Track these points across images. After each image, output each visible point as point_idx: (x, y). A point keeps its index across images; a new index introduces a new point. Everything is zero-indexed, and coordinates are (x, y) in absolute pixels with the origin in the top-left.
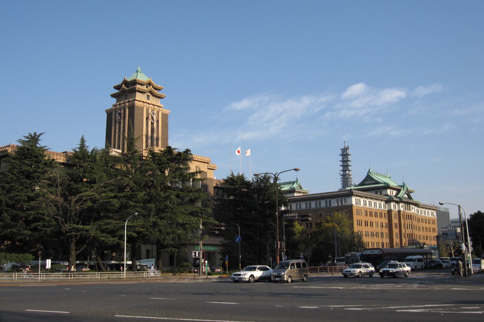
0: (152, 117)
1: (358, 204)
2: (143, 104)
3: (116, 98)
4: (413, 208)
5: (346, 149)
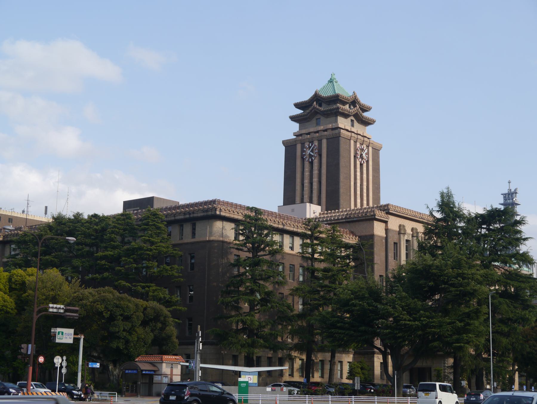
0: (361, 155)
2: (349, 134)
5: (513, 194)
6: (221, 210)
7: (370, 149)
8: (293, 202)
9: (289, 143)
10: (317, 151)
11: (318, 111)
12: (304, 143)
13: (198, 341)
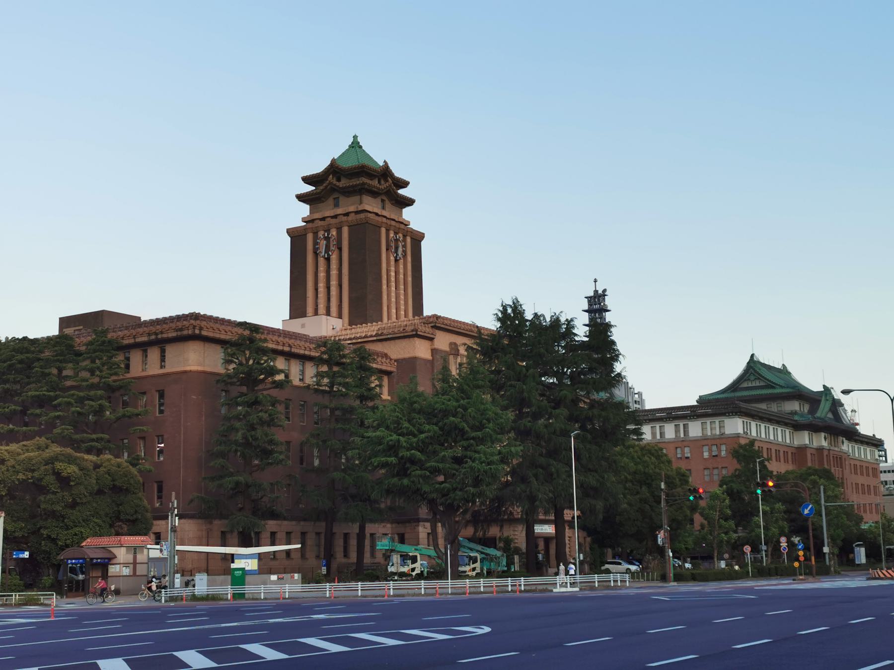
3: (307, 204)
4: (843, 442)
8: (303, 315)
9: (296, 232)
10: (335, 243)
11: (336, 188)
12: (317, 232)
13: (172, 514)
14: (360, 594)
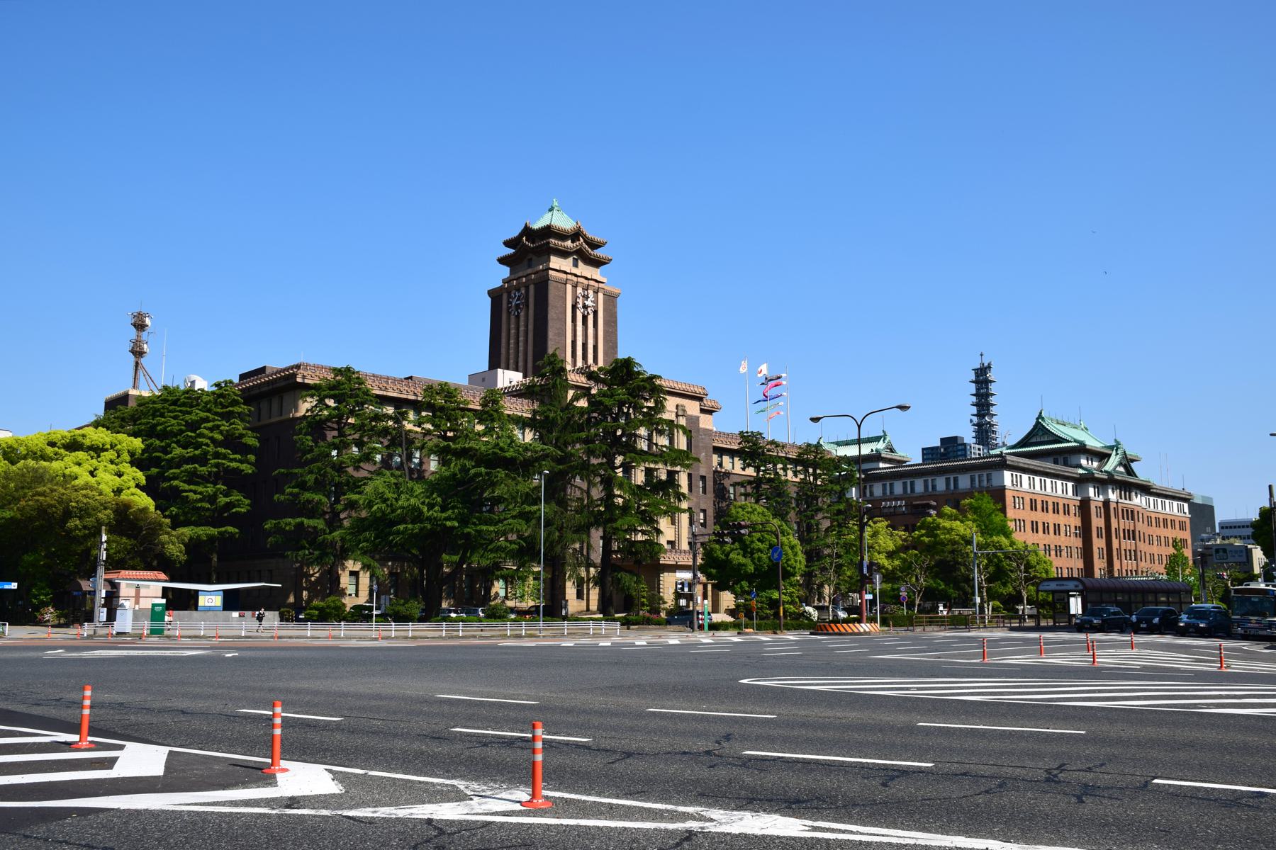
1: (1017, 485)
2: (564, 276)
3: (508, 266)
5: (986, 368)
6: (304, 377)
7: (601, 296)
14: (444, 635)
